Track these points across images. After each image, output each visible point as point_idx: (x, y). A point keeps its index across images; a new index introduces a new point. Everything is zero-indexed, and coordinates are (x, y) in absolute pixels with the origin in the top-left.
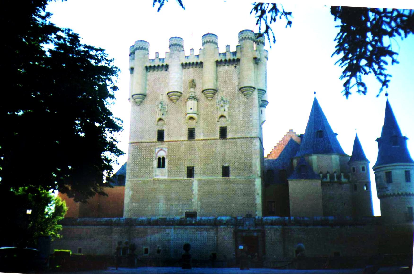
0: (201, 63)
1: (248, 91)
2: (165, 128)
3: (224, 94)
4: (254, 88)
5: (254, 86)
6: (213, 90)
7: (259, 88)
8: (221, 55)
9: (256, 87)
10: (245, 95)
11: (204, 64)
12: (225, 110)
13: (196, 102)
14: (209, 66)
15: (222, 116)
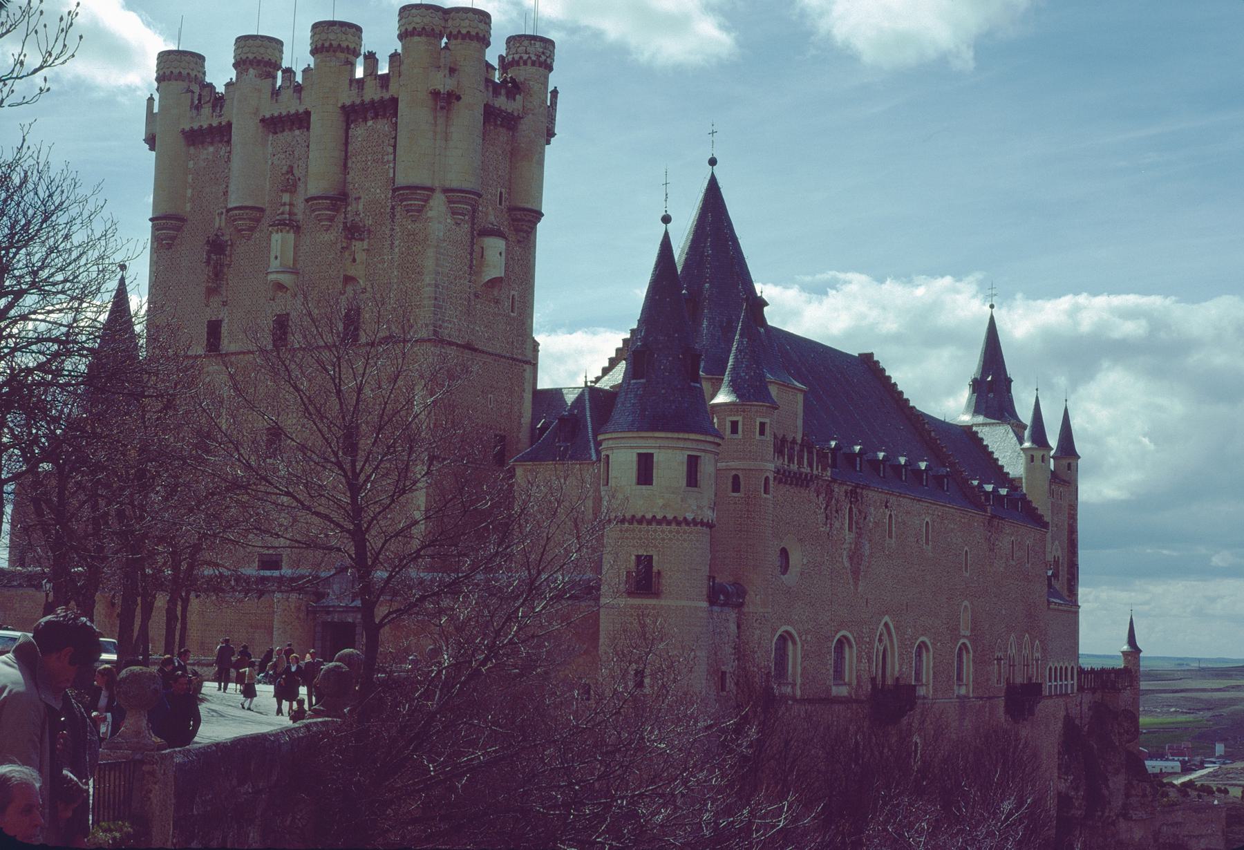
0: (308, 113)
1: (411, 199)
2: (223, 314)
3: (361, 207)
4: (432, 190)
5: (428, 183)
6: (326, 198)
7: (447, 186)
8: (354, 84)
9: (437, 184)
10: (408, 211)
11: (313, 118)
12: (354, 260)
13: (291, 236)
14: (324, 127)
15: (348, 279)
